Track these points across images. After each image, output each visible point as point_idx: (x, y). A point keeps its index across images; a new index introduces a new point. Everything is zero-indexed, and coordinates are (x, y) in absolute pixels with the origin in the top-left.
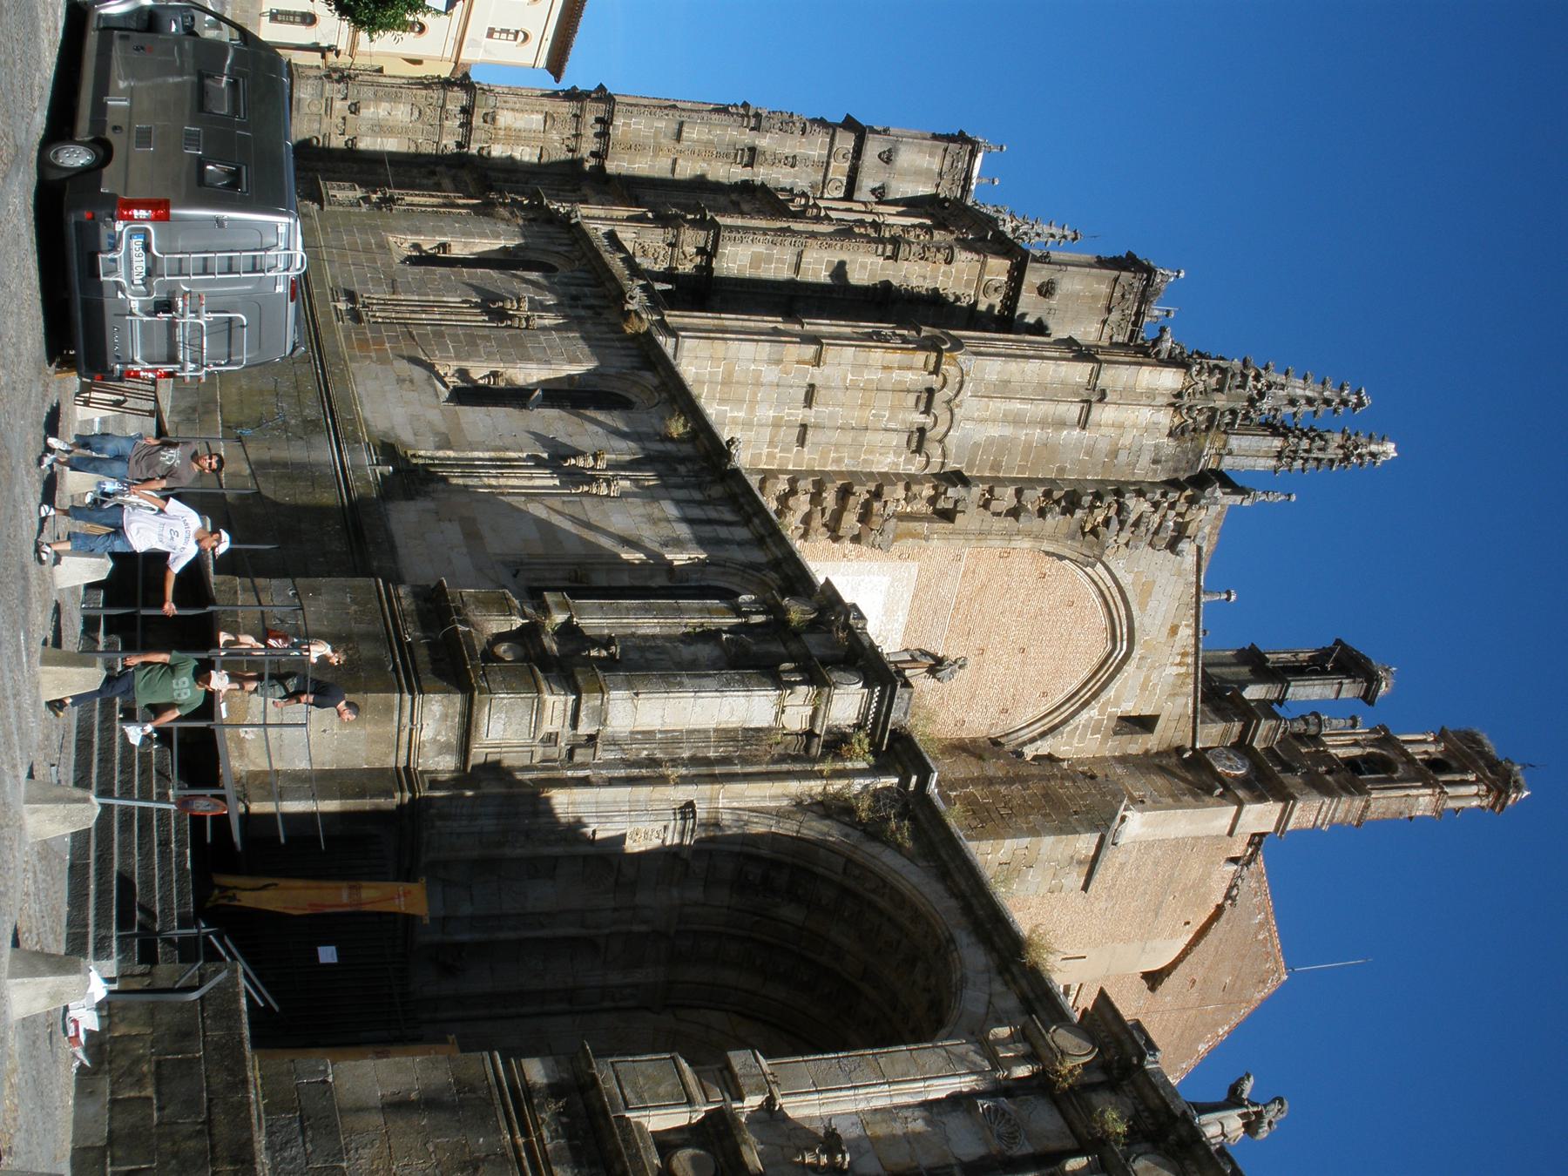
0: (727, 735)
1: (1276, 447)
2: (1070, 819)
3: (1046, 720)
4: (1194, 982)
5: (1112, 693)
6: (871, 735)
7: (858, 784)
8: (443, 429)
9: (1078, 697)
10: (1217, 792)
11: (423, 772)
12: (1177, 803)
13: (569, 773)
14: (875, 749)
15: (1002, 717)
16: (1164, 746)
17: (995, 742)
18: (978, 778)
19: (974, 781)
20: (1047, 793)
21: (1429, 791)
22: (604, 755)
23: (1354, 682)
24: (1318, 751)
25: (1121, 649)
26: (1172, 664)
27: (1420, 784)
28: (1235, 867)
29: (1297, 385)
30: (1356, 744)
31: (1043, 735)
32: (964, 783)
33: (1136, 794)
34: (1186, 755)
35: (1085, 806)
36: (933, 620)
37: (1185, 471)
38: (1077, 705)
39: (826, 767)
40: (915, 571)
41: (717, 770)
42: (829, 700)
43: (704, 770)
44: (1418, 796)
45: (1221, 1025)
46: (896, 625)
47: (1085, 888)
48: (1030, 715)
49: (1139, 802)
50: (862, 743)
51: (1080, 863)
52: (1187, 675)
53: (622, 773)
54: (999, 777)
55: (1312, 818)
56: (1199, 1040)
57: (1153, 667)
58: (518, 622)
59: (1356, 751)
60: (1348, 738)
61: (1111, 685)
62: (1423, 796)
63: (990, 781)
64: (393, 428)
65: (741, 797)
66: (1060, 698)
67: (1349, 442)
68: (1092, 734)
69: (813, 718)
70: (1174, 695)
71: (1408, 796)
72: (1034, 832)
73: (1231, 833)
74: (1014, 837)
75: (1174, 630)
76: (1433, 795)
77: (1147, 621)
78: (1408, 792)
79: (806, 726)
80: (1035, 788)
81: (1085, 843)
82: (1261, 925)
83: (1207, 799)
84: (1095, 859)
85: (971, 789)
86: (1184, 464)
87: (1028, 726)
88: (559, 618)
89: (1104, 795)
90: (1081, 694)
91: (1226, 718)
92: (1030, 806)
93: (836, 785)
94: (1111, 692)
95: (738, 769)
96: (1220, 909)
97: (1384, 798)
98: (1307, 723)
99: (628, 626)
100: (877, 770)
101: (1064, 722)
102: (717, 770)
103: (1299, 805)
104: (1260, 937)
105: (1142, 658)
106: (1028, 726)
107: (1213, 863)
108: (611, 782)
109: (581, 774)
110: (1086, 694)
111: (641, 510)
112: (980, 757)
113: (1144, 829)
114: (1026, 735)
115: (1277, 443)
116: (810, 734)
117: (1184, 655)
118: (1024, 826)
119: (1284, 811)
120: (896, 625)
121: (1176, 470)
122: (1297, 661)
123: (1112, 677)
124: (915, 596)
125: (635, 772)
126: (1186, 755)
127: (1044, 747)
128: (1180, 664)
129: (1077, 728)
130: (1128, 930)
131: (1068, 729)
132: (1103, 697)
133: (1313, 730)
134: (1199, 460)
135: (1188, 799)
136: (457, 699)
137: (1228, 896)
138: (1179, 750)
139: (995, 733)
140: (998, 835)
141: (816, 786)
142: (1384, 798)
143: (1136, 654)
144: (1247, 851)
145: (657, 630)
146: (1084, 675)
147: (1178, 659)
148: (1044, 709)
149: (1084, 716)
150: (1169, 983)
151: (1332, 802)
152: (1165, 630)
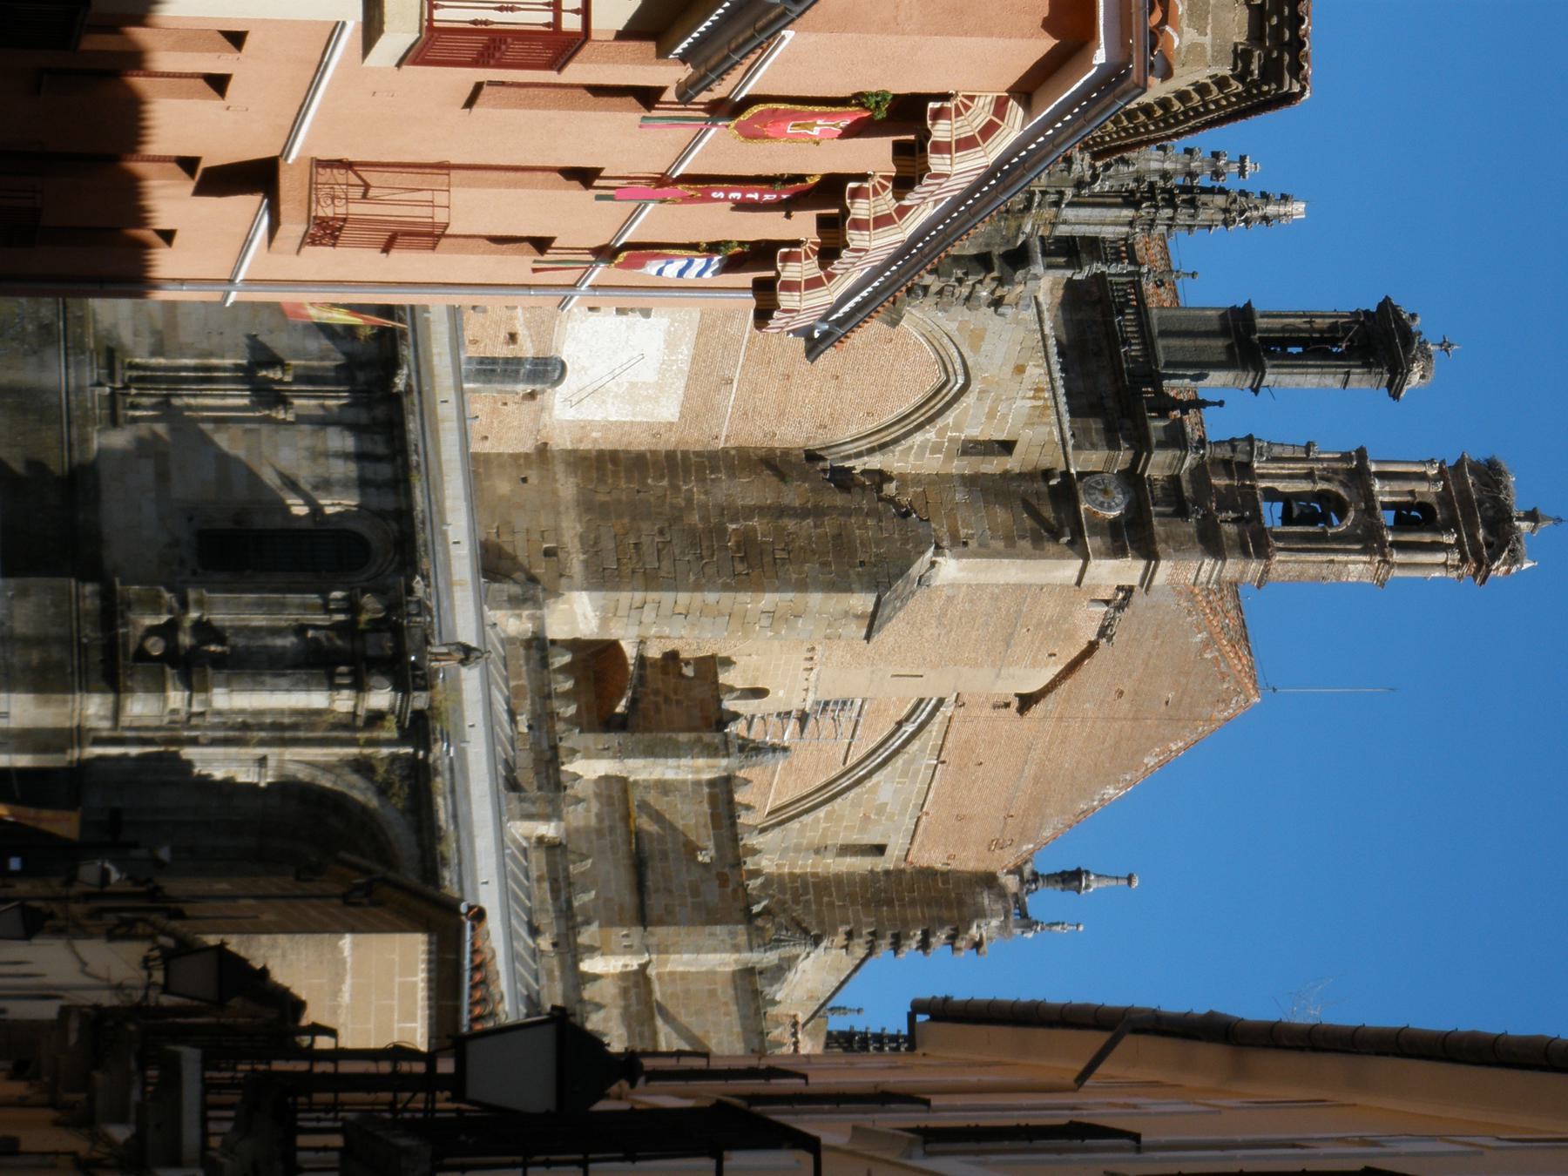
0: (296, 712)
1: (1127, 216)
2: (851, 572)
3: (873, 438)
4: (1121, 693)
5: (951, 420)
6: (399, 717)
7: (385, 751)
8: (159, 325)
9: (939, 397)
10: (1064, 540)
11: (91, 730)
12: (1009, 547)
13: (186, 734)
14: (400, 727)
15: (820, 431)
16: (1028, 468)
17: (812, 456)
18: (769, 508)
19: (761, 510)
20: (840, 535)
21: (1366, 558)
22: (210, 720)
23: (1370, 373)
24: (1244, 485)
25: (956, 382)
26: (1023, 398)
27: (1357, 547)
28: (1106, 609)
29: (1154, 157)
30: (1309, 476)
31: (871, 451)
32: (750, 512)
33: (963, 532)
34: (1053, 482)
35: (877, 555)
36: (723, 352)
37: (1000, 246)
38: (912, 426)
39: (362, 736)
40: (696, 315)
41: (288, 734)
42: (364, 699)
43: (278, 734)
44: (1346, 563)
45: (1174, 740)
46: (680, 357)
47: (868, 637)
48: (853, 431)
49: (960, 545)
50: (391, 722)
51: (857, 617)
52: (1045, 407)
53: (220, 734)
54: (794, 508)
55: (1192, 577)
56: (1146, 751)
57: (997, 400)
58: (164, 618)
59: (1304, 486)
60: (1300, 465)
61: (947, 413)
62: (1354, 562)
63: (780, 511)
64: (115, 326)
65: (300, 754)
66: (889, 418)
67: (1234, 206)
68: (930, 453)
69: (356, 706)
70: (1033, 424)
71: (1332, 562)
72: (802, 586)
73: (1079, 583)
74: (777, 590)
75: (1020, 370)
76: (1370, 563)
77: (982, 360)
78: (1332, 557)
79: (351, 709)
80: (829, 526)
81: (863, 602)
82: (1206, 645)
83: (1050, 547)
84: (874, 615)
85: (755, 522)
86: (998, 240)
87: (852, 441)
88: (194, 615)
89: (906, 542)
90: (913, 418)
91: (1113, 445)
92: (813, 550)
93: (368, 751)
94: (950, 418)
95: (301, 734)
96: (1092, 647)
97: (1295, 562)
98: (1234, 449)
99: (243, 620)
100: (403, 740)
101: (896, 441)
102: (288, 734)
103: (1163, 564)
104: (1208, 656)
105: (982, 392)
106: (852, 441)
107: (1073, 603)
108: (214, 742)
109: (193, 734)
110: (919, 418)
111: (307, 442)
112: (782, 477)
113: (962, 574)
114: (851, 449)
115: (1128, 213)
116: (354, 714)
117: (1037, 390)
118: (794, 576)
119: (1147, 569)
120: (680, 357)
121: (988, 245)
122: (1314, 330)
123: (949, 405)
124: (699, 334)
125: (231, 734)
126: (1053, 482)
127: (875, 462)
128: (1034, 398)
129: (911, 447)
130: (973, 655)
131: (900, 448)
132: (940, 423)
133: (1241, 457)
134: (1017, 237)
135: (1025, 544)
136: (110, 698)
137: (1102, 632)
138: (1047, 474)
139: (814, 444)
140: (759, 587)
141: (353, 751)
142: (1295, 562)
143: (975, 387)
144: (1117, 595)
145: (264, 623)
146: (917, 399)
147: (1031, 394)
148: (871, 426)
149: (918, 438)
150: (1037, 710)
151: (1216, 563)
152: (1009, 369)
